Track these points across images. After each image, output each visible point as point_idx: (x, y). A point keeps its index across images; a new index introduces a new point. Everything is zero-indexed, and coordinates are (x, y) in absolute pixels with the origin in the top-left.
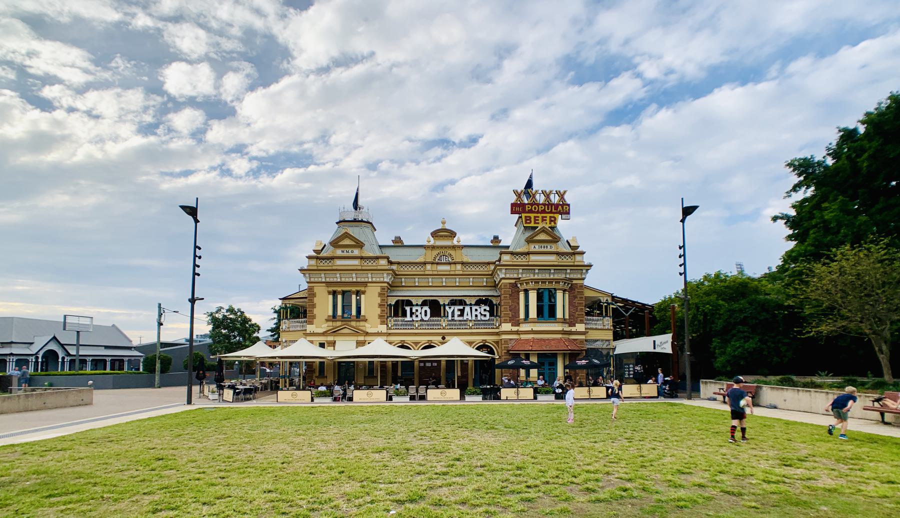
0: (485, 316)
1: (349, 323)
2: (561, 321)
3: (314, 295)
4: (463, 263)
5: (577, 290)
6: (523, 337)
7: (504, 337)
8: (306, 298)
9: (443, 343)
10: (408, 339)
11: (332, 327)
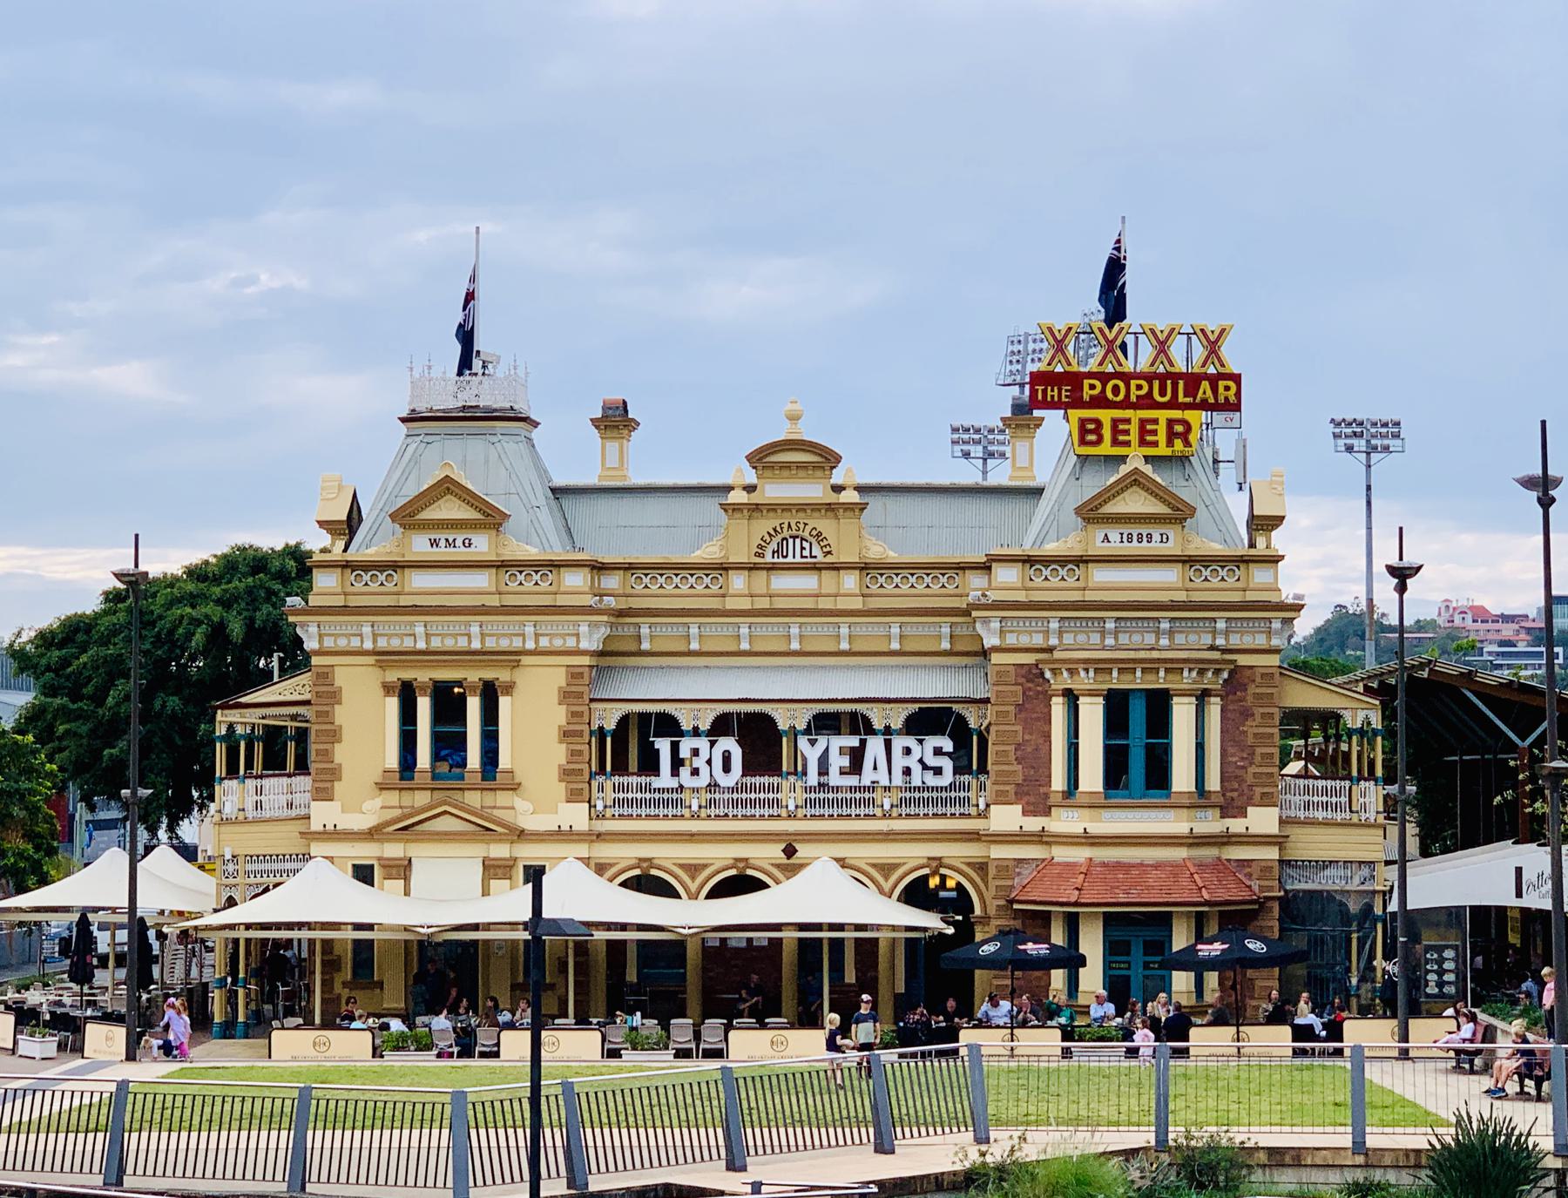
0: (938, 771)
1: (457, 795)
2: (1186, 801)
3: (334, 697)
4: (864, 568)
5: (1252, 689)
6: (1062, 854)
7: (999, 852)
8: (307, 703)
9: (791, 870)
10: (667, 856)
11: (397, 813)
